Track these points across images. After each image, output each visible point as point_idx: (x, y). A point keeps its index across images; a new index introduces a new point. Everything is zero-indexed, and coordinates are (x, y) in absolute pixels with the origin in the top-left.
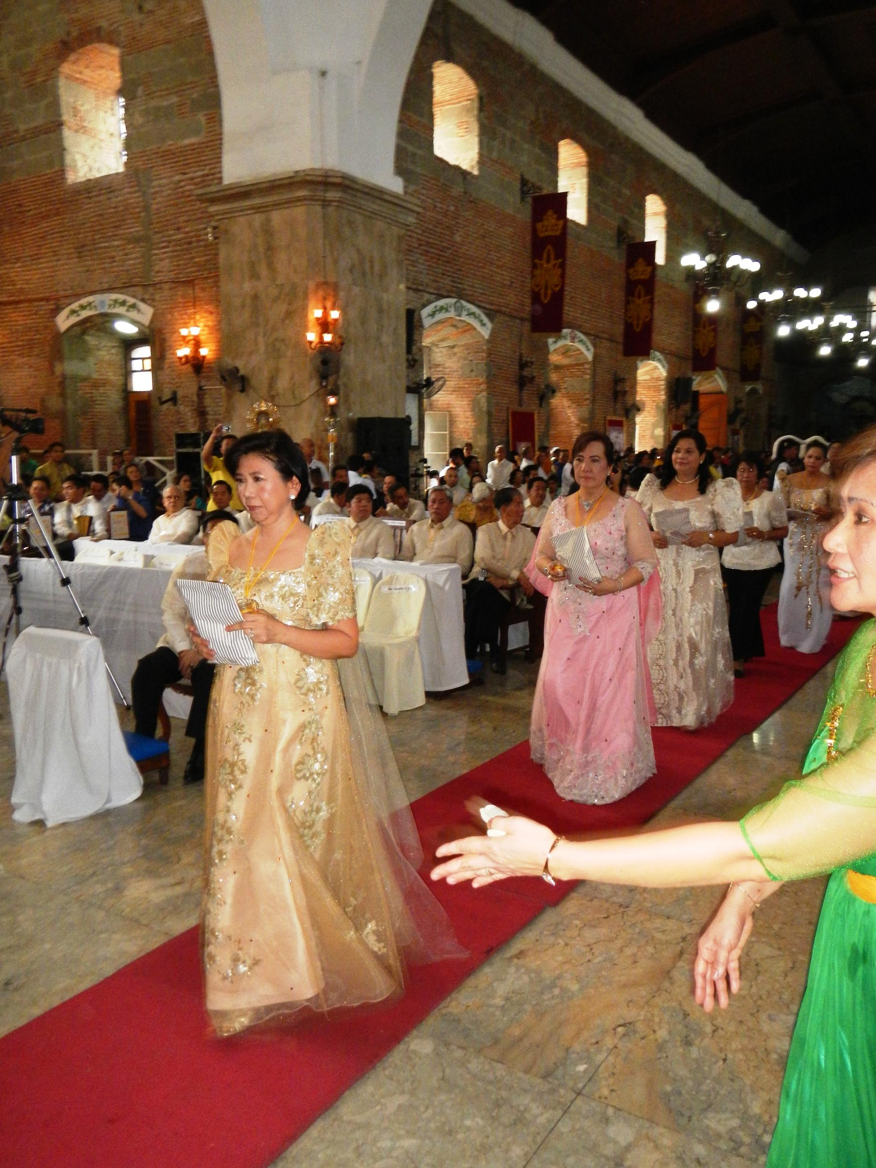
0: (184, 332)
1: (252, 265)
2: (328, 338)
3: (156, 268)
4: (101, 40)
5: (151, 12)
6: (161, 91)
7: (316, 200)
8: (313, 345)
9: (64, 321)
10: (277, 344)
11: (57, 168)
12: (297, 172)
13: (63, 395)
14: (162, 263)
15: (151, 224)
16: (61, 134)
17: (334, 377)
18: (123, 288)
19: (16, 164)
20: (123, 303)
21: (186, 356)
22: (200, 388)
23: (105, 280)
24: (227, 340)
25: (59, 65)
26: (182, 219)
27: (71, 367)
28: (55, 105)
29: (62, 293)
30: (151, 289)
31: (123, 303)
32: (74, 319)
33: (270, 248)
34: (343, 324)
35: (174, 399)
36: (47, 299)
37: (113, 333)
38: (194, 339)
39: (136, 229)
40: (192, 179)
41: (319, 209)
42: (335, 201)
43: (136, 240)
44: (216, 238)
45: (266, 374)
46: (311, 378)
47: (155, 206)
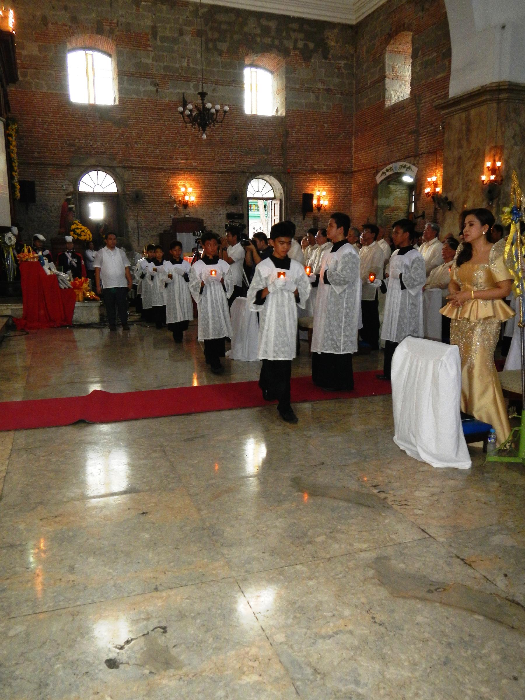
0: (429, 179)
1: (460, 140)
2: (493, 177)
3: (420, 147)
4: (404, 30)
5: (428, 9)
6: (429, 51)
7: (494, 100)
8: (485, 183)
9: (379, 178)
10: (468, 184)
11: (382, 100)
12: (482, 87)
13: (376, 216)
14: (423, 144)
15: (420, 123)
16: (385, 82)
17: (497, 199)
18: (406, 158)
19: (365, 101)
20: (405, 167)
21: (428, 193)
22: (436, 209)
23: (398, 155)
24: (447, 182)
25: (386, 47)
26: (434, 118)
27: (381, 201)
28: (383, 69)
29: (379, 164)
30: (417, 158)
31: (405, 167)
32: (384, 177)
33: (469, 130)
34: (505, 170)
35: (423, 216)
36: (373, 168)
37: (402, 183)
38: (434, 183)
39: (412, 127)
40: (440, 96)
41: (495, 105)
42: (504, 99)
43: (412, 133)
44: (443, 128)
45: (462, 200)
46: (483, 201)
47: (422, 114)
